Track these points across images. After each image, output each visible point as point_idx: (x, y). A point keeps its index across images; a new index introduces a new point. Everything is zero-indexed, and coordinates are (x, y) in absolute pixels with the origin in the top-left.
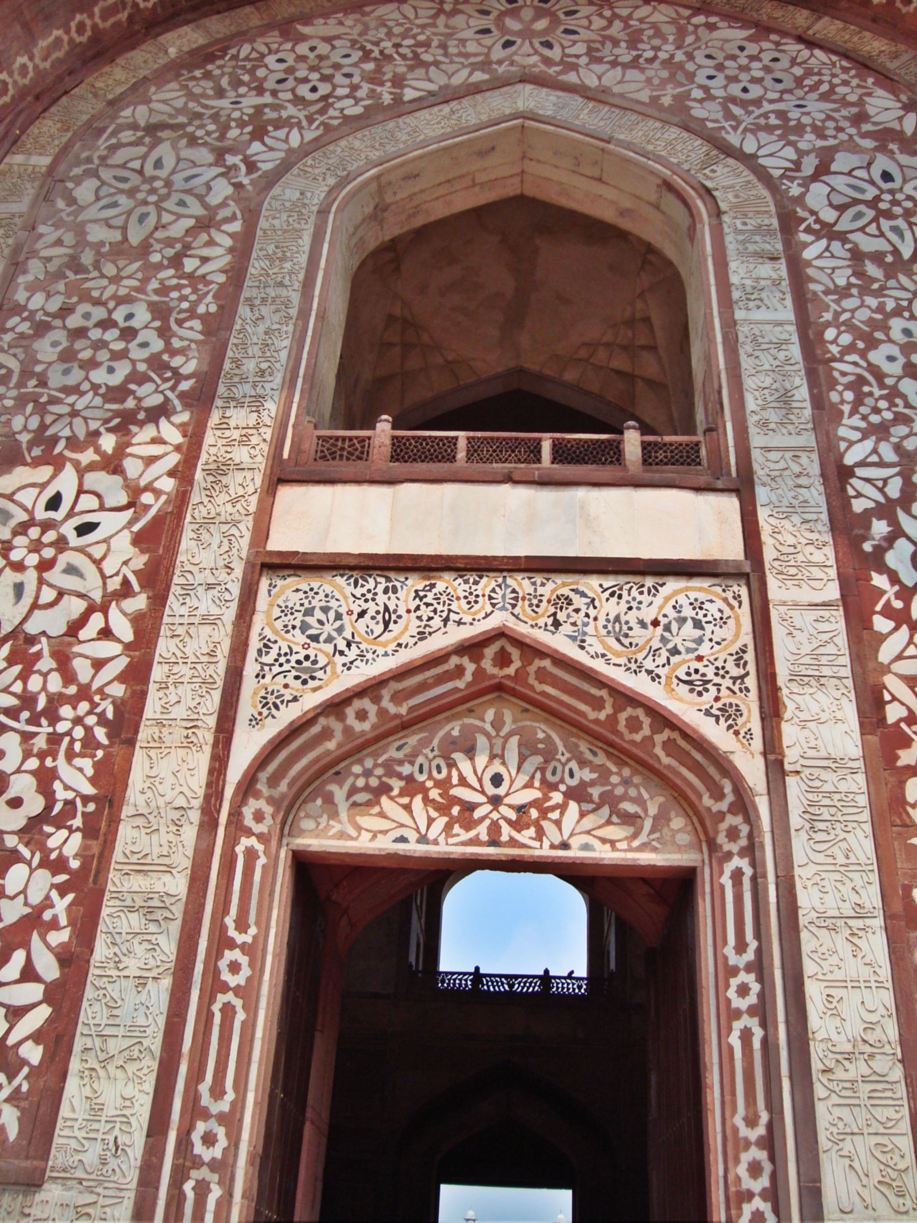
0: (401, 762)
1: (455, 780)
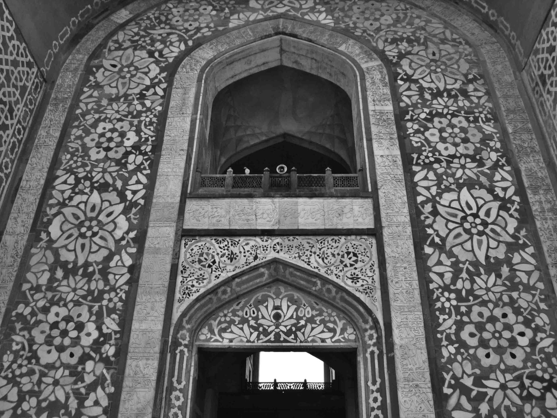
0: (238, 311)
1: (260, 317)
